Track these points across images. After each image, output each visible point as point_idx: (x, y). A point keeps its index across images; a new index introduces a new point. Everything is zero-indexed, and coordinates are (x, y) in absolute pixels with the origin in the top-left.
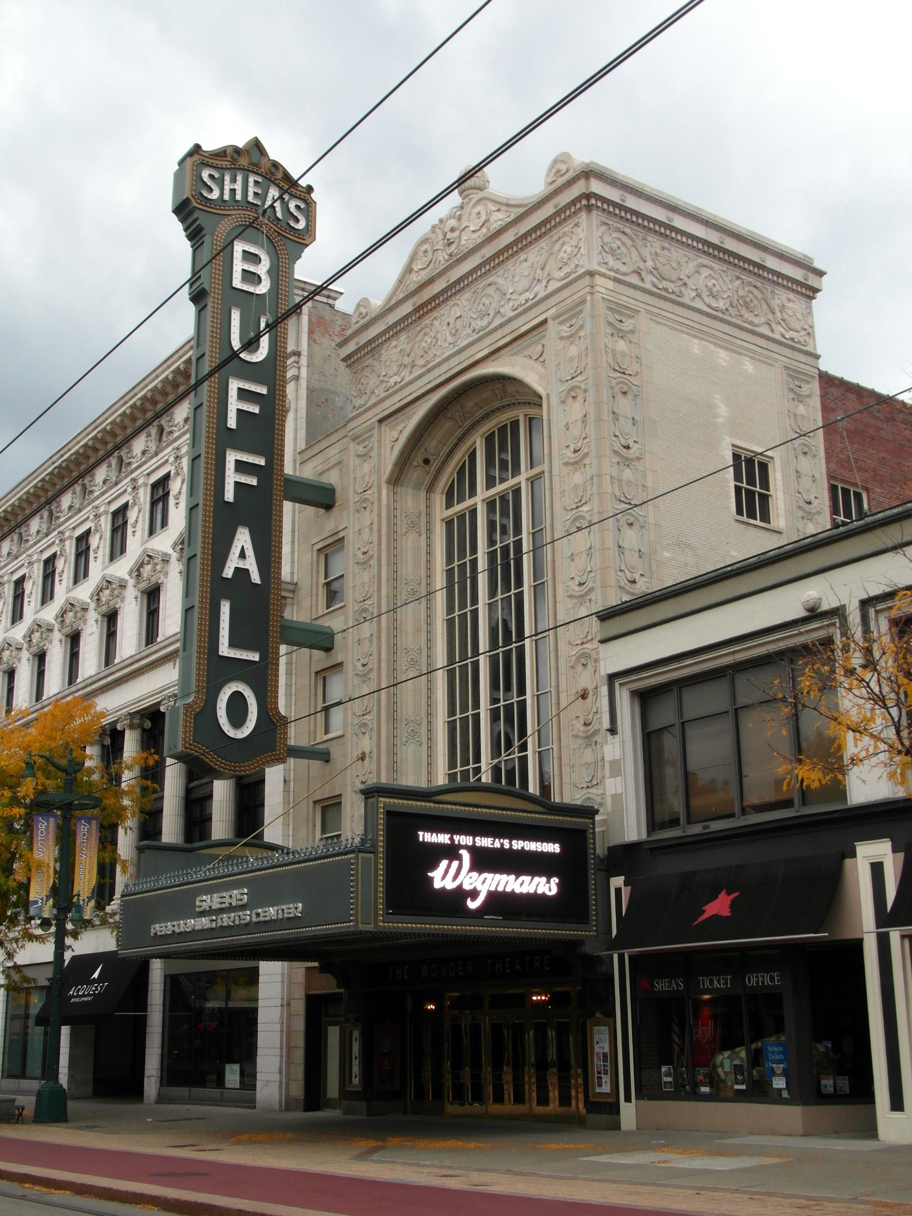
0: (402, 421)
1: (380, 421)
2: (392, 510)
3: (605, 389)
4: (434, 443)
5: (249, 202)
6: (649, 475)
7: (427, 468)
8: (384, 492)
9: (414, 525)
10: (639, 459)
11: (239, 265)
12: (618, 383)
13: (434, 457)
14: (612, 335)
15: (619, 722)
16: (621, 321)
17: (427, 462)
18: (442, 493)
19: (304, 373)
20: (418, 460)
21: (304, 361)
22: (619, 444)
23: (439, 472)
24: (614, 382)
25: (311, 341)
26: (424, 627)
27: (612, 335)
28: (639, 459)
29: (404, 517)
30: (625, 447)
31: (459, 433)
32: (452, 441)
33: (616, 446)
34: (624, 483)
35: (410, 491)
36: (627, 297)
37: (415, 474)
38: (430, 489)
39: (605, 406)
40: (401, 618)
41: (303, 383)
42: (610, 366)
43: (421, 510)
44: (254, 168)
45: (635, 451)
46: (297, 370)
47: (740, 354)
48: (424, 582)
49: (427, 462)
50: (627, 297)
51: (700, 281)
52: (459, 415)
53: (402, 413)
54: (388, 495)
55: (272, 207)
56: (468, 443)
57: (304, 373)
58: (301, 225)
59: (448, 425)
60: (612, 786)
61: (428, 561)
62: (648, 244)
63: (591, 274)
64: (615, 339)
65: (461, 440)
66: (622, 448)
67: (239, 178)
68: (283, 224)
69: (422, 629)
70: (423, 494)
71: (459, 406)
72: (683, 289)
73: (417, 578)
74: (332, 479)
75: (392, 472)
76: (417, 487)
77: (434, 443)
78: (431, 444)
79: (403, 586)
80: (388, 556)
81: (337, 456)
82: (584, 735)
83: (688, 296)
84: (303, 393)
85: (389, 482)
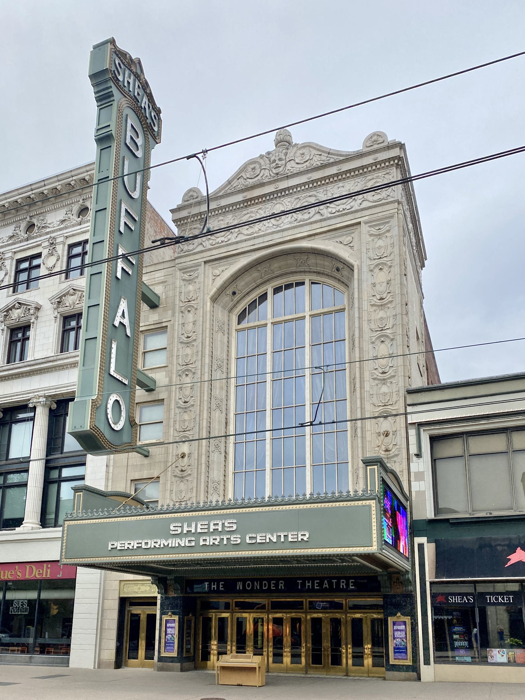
0: (224, 265)
4: (243, 283)
13: (239, 292)
31: (259, 281)
32: (254, 285)
53: (225, 260)
56: (265, 288)
59: (255, 274)
71: (268, 265)
75: (215, 293)
77: (243, 283)
79: (215, 361)
81: (163, 278)
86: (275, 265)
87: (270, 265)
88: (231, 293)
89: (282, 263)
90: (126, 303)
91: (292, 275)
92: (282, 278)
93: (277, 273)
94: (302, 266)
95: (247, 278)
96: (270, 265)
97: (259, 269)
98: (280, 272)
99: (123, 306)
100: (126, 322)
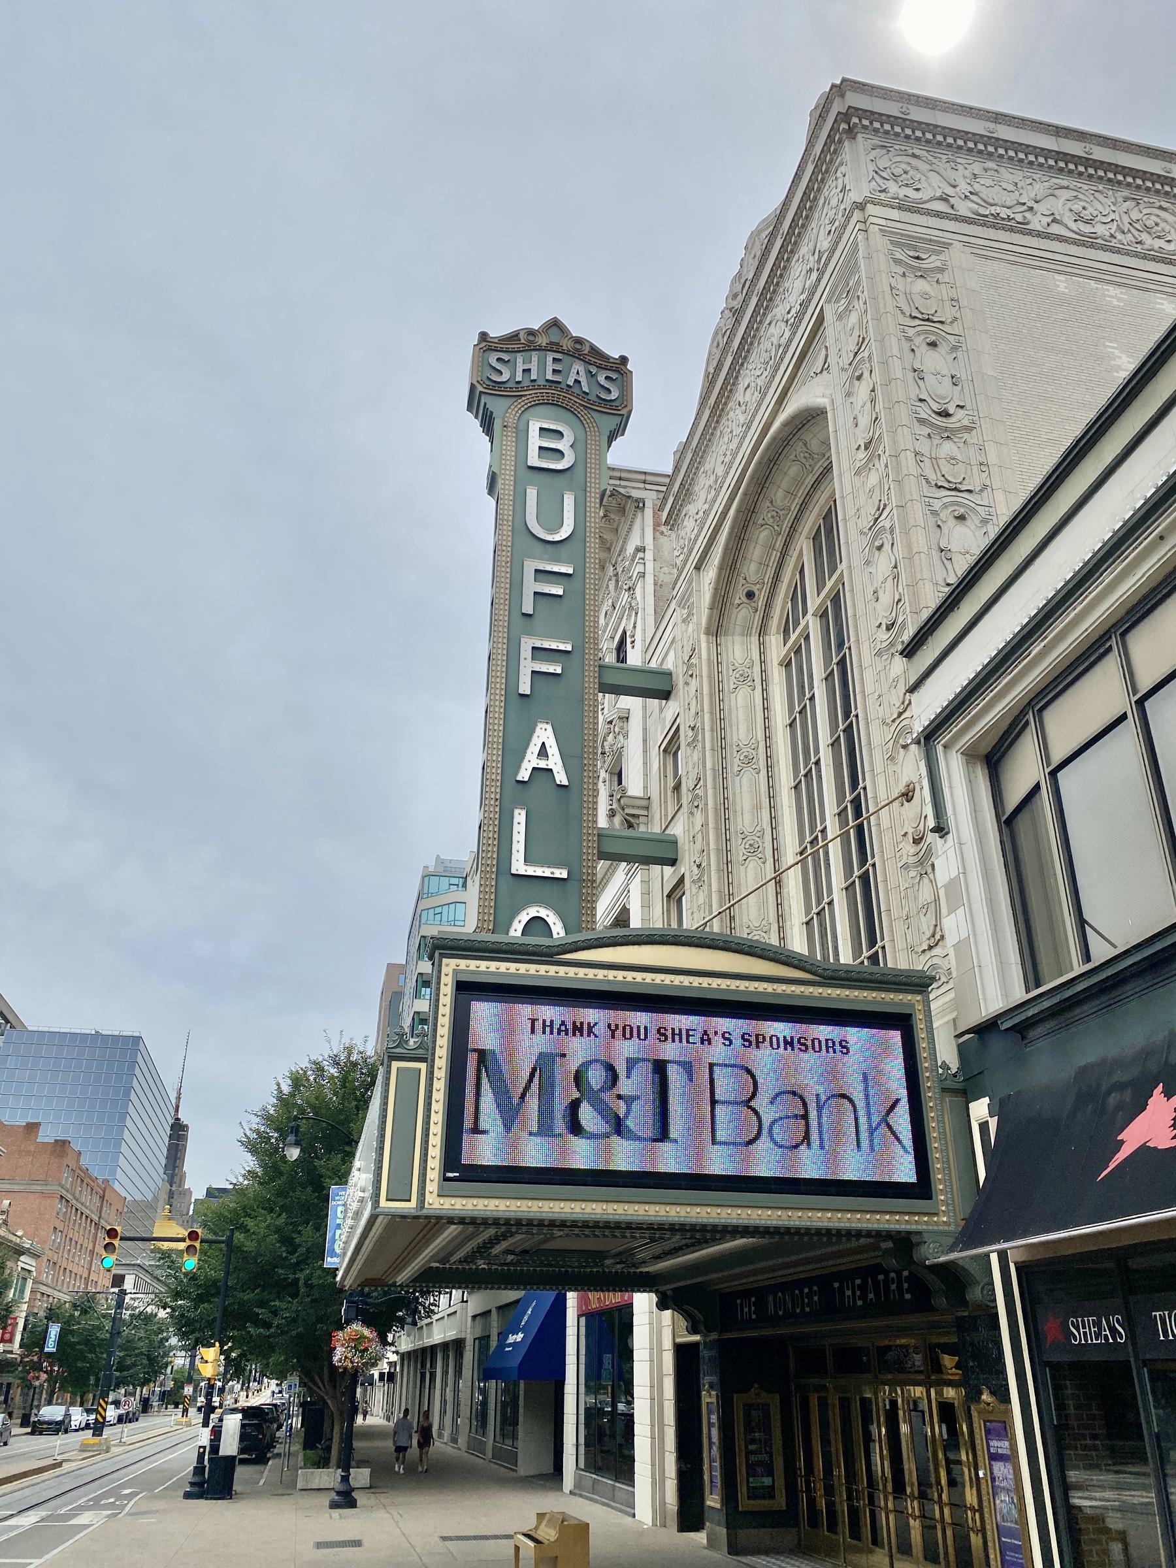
1: (698, 568)
2: (717, 663)
3: (894, 340)
5: (548, 381)
6: (991, 449)
7: (753, 605)
8: (704, 645)
9: (745, 678)
10: (969, 429)
11: (535, 441)
12: (919, 334)
14: (904, 275)
15: (950, 812)
16: (918, 258)
17: (750, 595)
18: (778, 633)
19: (650, 566)
20: (739, 596)
21: (649, 555)
22: (930, 412)
23: (768, 605)
24: (911, 332)
25: (658, 534)
26: (765, 801)
27: (904, 275)
28: (969, 429)
29: (731, 671)
30: (939, 414)
31: (779, 544)
32: (776, 555)
33: (922, 412)
34: (942, 462)
35: (738, 639)
36: (920, 225)
37: (741, 615)
38: (763, 631)
39: (897, 362)
40: (734, 794)
41: (649, 579)
42: (903, 313)
43: (754, 658)
44: (553, 347)
45: (959, 418)
46: (642, 566)
47: (1147, 290)
48: (762, 744)
49: (750, 595)
50: (920, 225)
51: (1059, 205)
52: (773, 517)
54: (709, 648)
55: (577, 382)
57: (650, 566)
58: (614, 395)
59: (764, 535)
60: (954, 925)
61: (766, 718)
62: (959, 167)
63: (861, 206)
64: (909, 280)
65: (784, 554)
66: (933, 415)
67: (535, 359)
68: (592, 397)
69: (764, 805)
70: (754, 639)
71: (769, 505)
72: (1028, 215)
73: (753, 741)
74: (669, 665)
76: (746, 632)
78: (752, 570)
80: (712, 721)
82: (916, 859)
83: (1037, 223)
84: (650, 588)
85: (707, 633)
86: (778, 494)
87: (771, 502)
88: (744, 599)
89: (785, 484)
90: (549, 727)
91: (820, 492)
92: (810, 508)
93: (795, 508)
94: (816, 463)
95: (755, 552)
96: (771, 502)
97: (760, 521)
98: (796, 501)
99: (544, 734)
100: (554, 762)
